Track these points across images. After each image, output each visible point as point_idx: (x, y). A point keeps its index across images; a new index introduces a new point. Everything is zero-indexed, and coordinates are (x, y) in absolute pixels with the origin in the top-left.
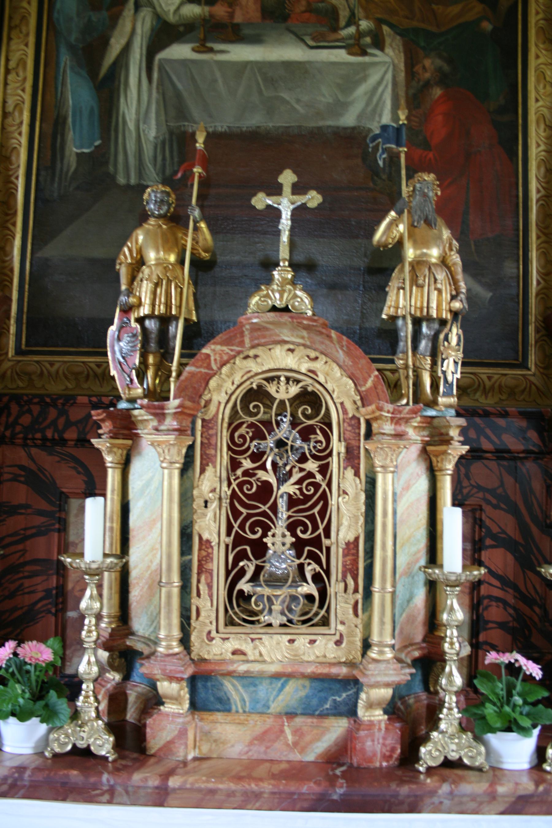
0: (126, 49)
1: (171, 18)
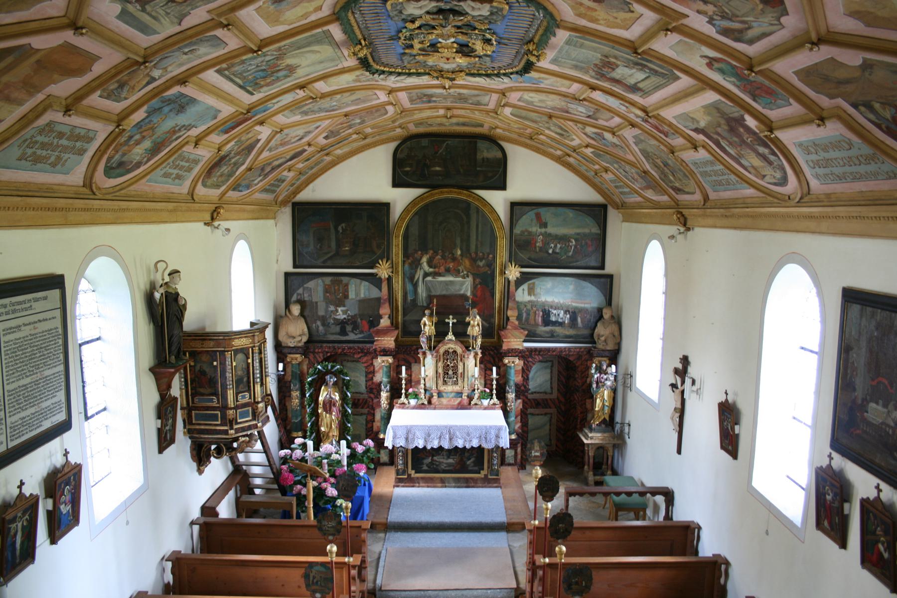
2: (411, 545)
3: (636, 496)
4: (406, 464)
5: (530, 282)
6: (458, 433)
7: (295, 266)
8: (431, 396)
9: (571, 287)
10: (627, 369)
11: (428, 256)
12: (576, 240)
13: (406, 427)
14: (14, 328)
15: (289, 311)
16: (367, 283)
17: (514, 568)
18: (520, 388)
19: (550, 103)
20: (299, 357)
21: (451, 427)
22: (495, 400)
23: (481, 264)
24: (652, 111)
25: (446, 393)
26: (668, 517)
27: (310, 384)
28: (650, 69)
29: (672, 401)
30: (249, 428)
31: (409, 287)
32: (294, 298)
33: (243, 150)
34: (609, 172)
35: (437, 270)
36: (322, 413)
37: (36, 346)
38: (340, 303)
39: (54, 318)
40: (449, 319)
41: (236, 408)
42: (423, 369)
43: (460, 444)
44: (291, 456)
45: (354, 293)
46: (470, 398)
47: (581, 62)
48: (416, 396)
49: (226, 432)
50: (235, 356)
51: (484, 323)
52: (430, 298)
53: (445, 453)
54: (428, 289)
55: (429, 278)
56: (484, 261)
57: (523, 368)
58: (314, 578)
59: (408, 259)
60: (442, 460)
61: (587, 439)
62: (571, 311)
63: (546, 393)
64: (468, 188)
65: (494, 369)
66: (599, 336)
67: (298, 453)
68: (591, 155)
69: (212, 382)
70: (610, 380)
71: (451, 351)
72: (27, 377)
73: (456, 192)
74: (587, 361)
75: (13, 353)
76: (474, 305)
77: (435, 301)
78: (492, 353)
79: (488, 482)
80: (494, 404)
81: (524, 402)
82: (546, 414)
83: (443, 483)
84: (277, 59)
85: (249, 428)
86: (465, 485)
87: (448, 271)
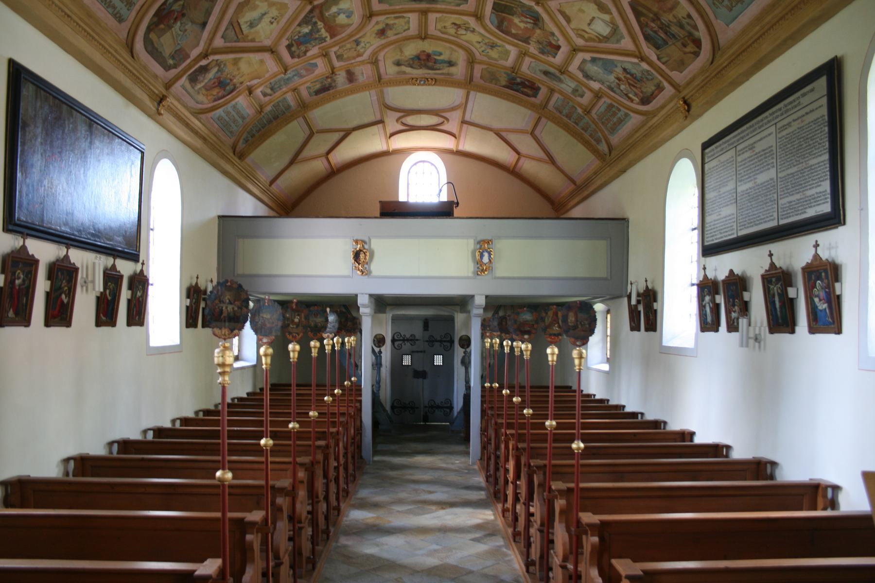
14: (785, 125)
37: (803, 137)
39: (822, 105)
72: (794, 166)
75: (785, 146)
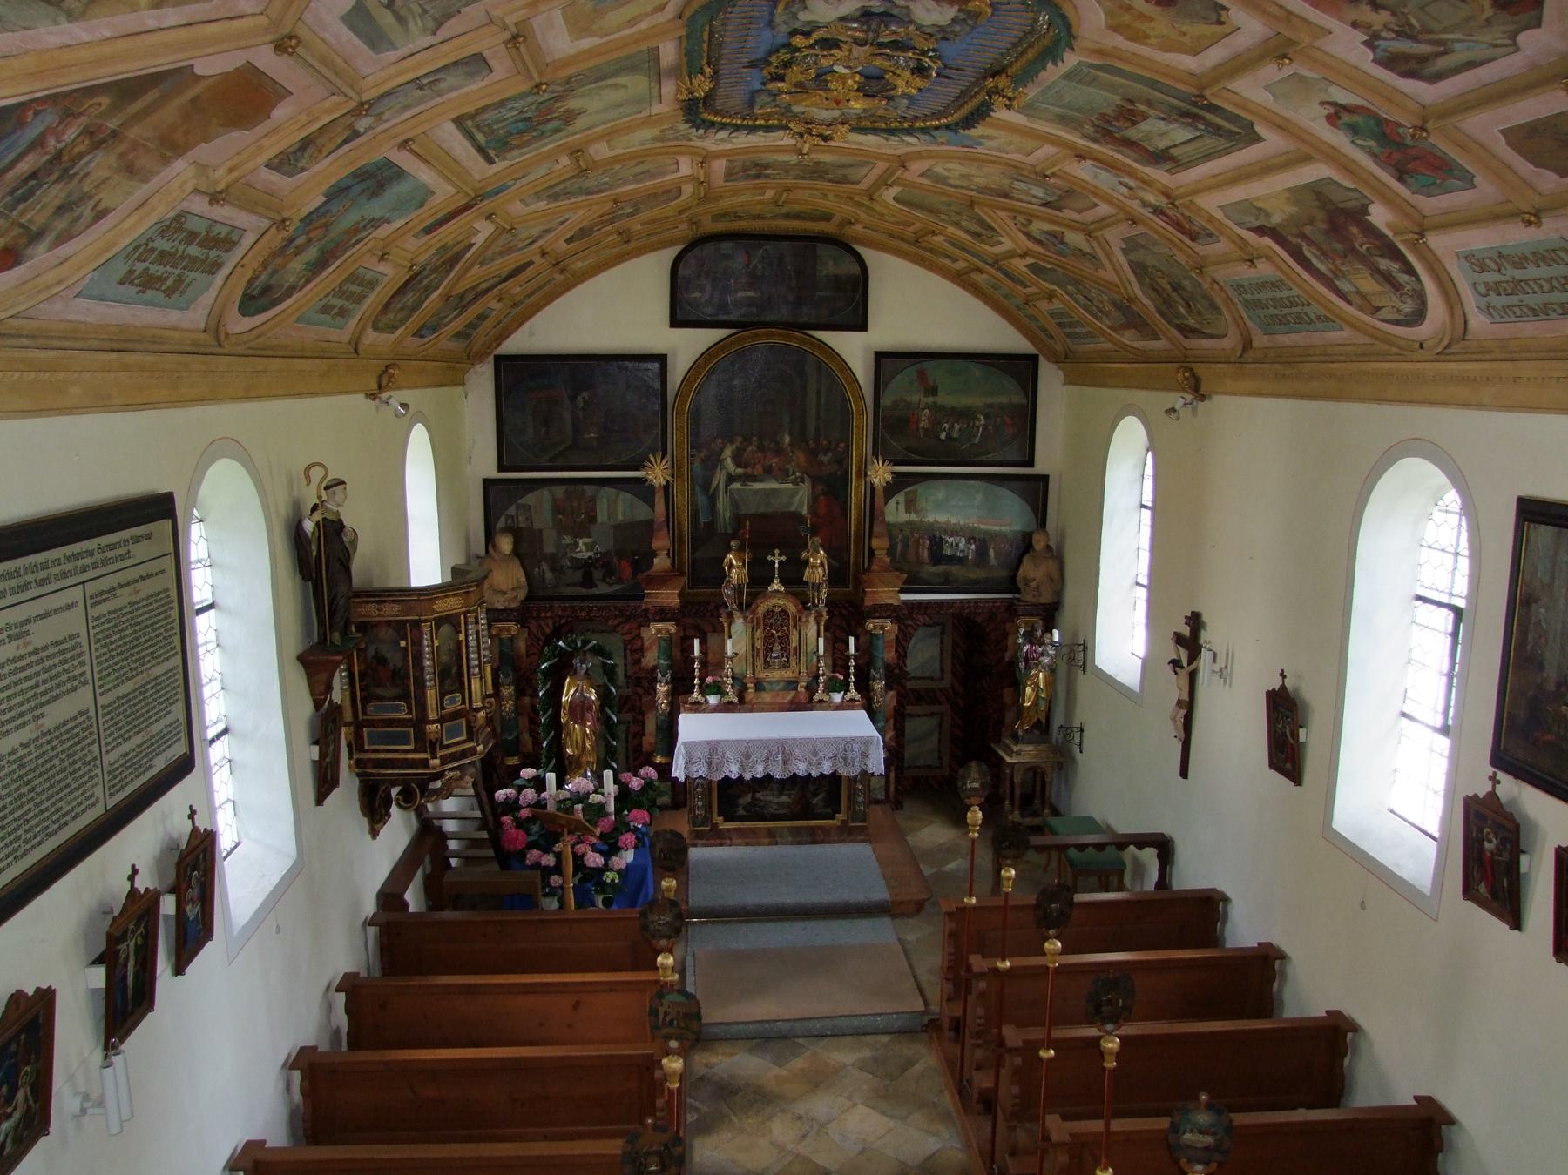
0: (717, 487)
1: (733, 474)
2: (734, 946)
3: (1111, 850)
4: (708, 807)
5: (908, 489)
6: (797, 752)
7: (501, 468)
8: (744, 688)
9: (979, 497)
10: (1075, 635)
11: (734, 446)
12: (987, 417)
13: (709, 743)
14: (106, 592)
15: (494, 546)
16: (628, 496)
17: (915, 977)
18: (893, 671)
19: (980, 181)
20: (514, 627)
21: (786, 741)
22: (853, 693)
23: (825, 459)
24: (1182, 197)
25: (770, 682)
26: (1163, 883)
27: (546, 672)
28: (1208, 124)
29: (1173, 688)
30: (464, 754)
31: (702, 500)
32: (501, 523)
33: (443, 263)
34: (1054, 300)
35: (749, 470)
36: (567, 724)
37: (139, 623)
38: (581, 531)
39: (162, 572)
40: (774, 555)
41: (441, 720)
42: (729, 643)
43: (801, 769)
44: (517, 799)
45: (605, 513)
46: (811, 689)
47: (1078, 110)
48: (718, 689)
49: (425, 763)
50: (438, 628)
51: (831, 560)
52: (738, 520)
53: (775, 786)
54: (735, 505)
55: (736, 485)
56: (830, 454)
57: (897, 637)
58: (666, 1014)
59: (700, 452)
60: (769, 798)
61: (1010, 756)
62: (977, 537)
63: (932, 679)
64: (801, 327)
65: (852, 640)
66: (1027, 582)
67: (529, 794)
68: (1025, 269)
69: (398, 676)
70: (1048, 655)
71: (777, 610)
72: (128, 679)
73: (780, 335)
74: (1004, 623)
75: (107, 637)
76: (814, 531)
77: (748, 523)
78: (844, 612)
79: (847, 833)
80: (852, 700)
81: (899, 695)
82: (932, 714)
83: (773, 837)
84: (556, 99)
85: (464, 754)
86: (809, 839)
87: (768, 472)
